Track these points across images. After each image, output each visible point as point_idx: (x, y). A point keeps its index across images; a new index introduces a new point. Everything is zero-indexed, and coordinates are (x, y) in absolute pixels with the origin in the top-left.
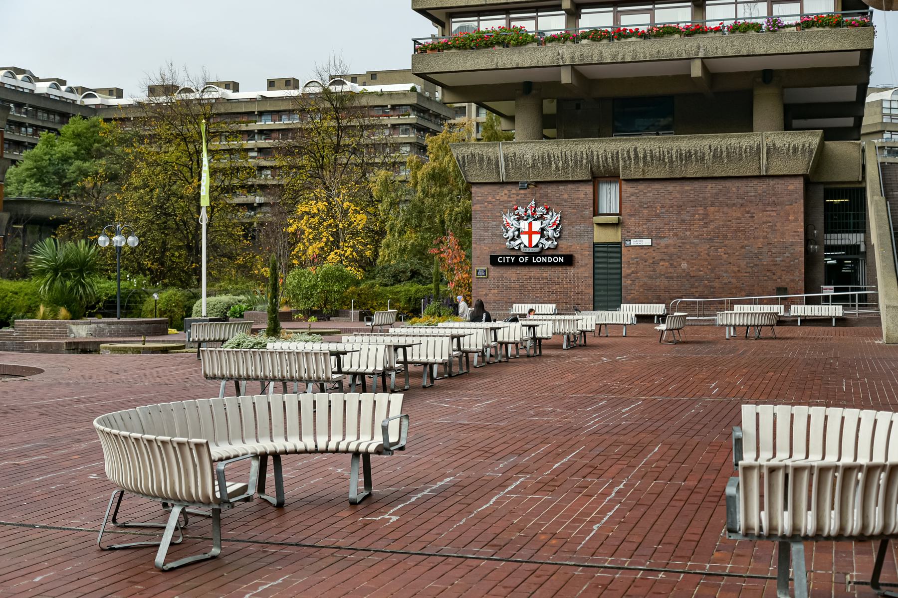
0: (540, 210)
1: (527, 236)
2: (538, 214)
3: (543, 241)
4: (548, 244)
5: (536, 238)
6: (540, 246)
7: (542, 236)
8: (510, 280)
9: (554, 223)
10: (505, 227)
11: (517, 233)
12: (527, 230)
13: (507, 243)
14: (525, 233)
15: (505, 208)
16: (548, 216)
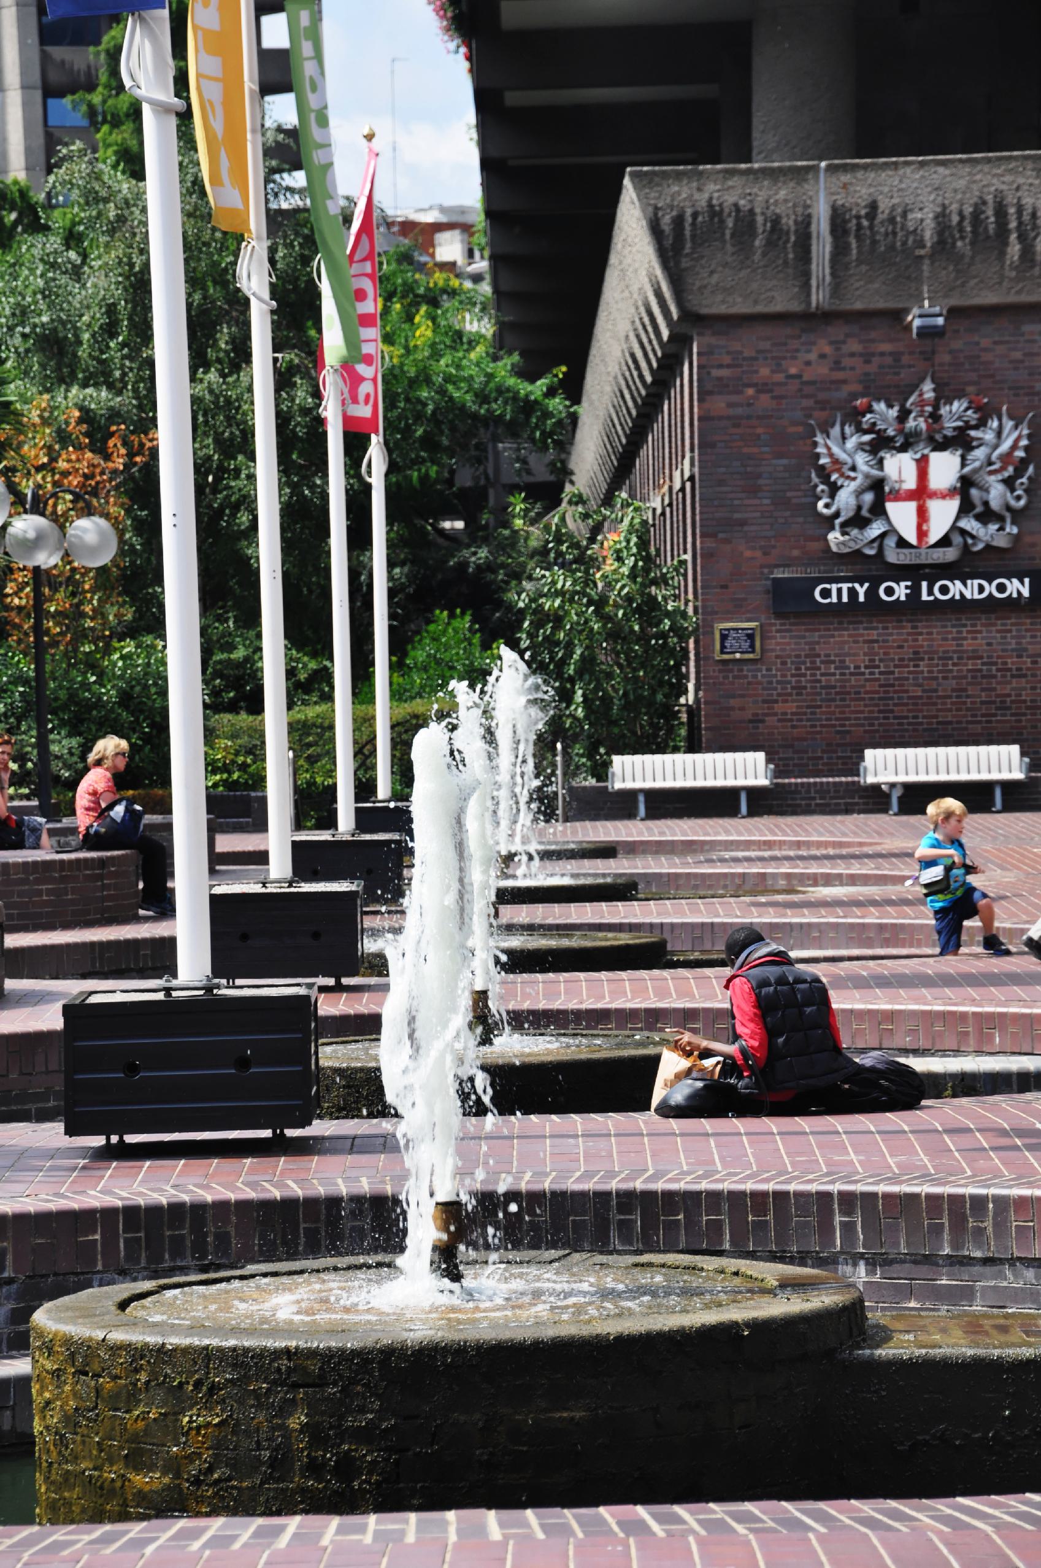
0: (955, 412)
1: (912, 506)
2: (950, 425)
3: (969, 524)
4: (985, 533)
5: (943, 515)
6: (957, 539)
7: (966, 508)
8: (842, 665)
9: (1006, 458)
10: (824, 474)
11: (869, 497)
12: (911, 483)
13: (834, 537)
14: (898, 496)
15: (823, 405)
16: (989, 436)
